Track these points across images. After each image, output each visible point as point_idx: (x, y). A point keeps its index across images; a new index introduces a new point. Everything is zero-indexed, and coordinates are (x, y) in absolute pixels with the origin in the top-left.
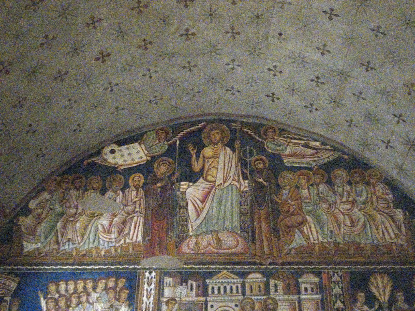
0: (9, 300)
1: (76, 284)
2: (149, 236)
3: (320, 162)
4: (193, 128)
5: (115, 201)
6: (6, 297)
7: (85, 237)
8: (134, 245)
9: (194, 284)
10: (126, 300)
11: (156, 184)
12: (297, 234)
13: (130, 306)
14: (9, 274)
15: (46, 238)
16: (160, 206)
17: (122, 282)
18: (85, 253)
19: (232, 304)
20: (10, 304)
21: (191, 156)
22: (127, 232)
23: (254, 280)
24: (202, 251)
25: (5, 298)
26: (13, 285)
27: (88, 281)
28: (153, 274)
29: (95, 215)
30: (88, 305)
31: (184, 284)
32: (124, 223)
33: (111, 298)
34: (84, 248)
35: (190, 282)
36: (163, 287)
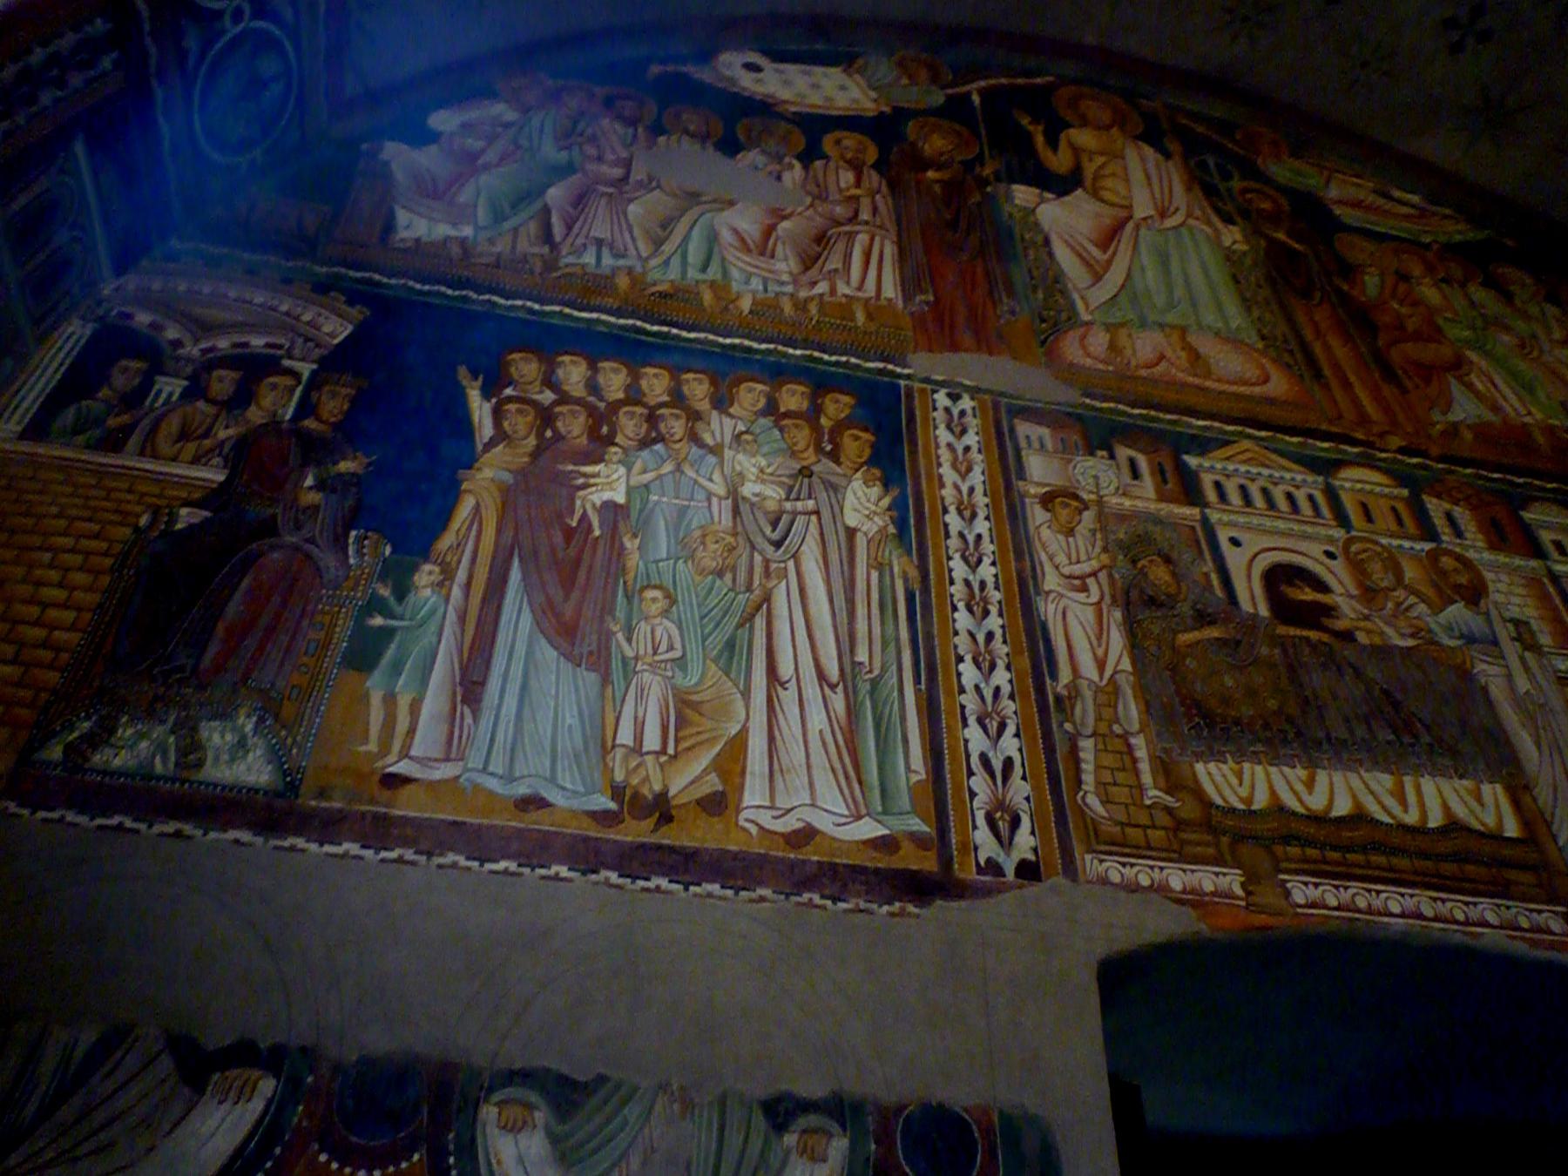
0: (306, 375)
1: (635, 376)
5: (779, 178)
6: (290, 357)
7: (668, 248)
8: (875, 309)
9: (1143, 462)
10: (872, 461)
11: (926, 170)
13: (886, 485)
14: (322, 288)
15: (498, 217)
16: (953, 225)
17: (837, 406)
18: (671, 291)
19: (1317, 549)
20: (315, 383)
21: (1028, 138)
22: (834, 263)
23: (1368, 487)
24: (1143, 373)
25: (287, 363)
26: (336, 329)
27: (690, 376)
28: (966, 403)
29: (704, 199)
31: (1104, 453)
32: (821, 239)
33: (801, 446)
34: (663, 275)
36: (1018, 451)
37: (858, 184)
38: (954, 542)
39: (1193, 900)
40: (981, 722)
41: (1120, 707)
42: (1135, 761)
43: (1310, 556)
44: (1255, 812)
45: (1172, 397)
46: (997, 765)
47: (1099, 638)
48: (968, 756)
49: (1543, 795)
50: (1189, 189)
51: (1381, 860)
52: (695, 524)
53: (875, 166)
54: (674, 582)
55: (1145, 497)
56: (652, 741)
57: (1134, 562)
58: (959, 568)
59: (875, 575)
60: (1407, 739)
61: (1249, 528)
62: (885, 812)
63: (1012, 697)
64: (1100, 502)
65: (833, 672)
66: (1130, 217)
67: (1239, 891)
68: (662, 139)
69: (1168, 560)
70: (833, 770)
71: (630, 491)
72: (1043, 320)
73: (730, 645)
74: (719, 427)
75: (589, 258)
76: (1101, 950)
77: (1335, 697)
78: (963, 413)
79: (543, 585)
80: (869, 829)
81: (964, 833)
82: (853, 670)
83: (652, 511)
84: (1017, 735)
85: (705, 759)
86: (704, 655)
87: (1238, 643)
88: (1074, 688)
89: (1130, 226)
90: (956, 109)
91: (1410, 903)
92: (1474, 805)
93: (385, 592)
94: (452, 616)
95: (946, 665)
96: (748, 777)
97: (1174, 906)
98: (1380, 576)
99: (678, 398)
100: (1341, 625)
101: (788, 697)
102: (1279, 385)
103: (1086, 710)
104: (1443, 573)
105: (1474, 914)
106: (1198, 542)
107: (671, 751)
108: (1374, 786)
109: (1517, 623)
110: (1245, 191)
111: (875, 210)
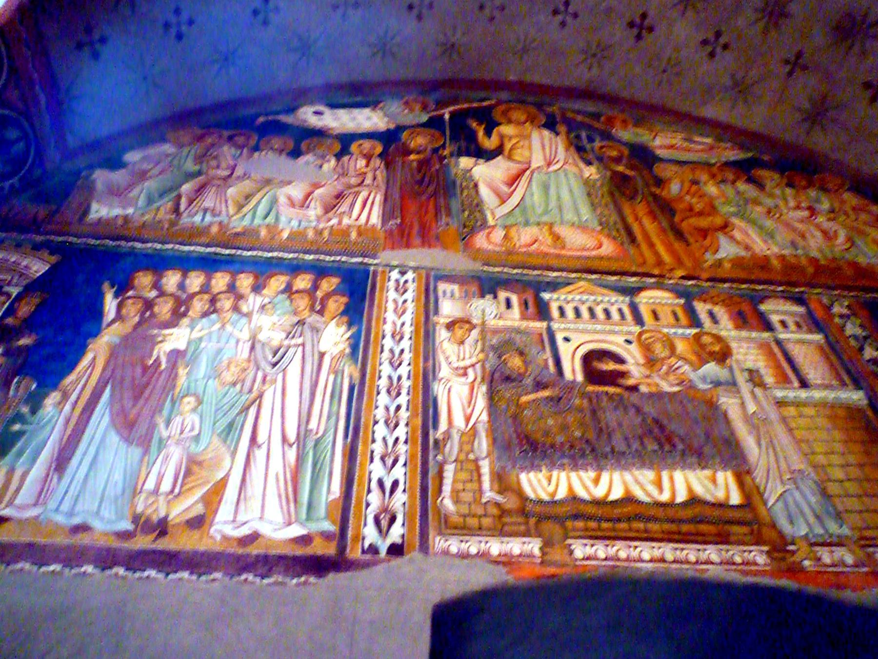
1: (209, 278)
2: (393, 217)
3: (724, 160)
4: (475, 105)
5: (321, 167)
7: (245, 210)
9: (514, 299)
12: (723, 240)
13: (350, 325)
15: (150, 201)
16: (420, 182)
19: (620, 339)
22: (344, 207)
26: (38, 267)
28: (410, 275)
30: (235, 316)
32: (339, 196)
34: (238, 224)
35: (503, 295)
37: (367, 166)
38: (386, 355)
39: (506, 561)
40: (383, 459)
41: (476, 443)
42: (480, 475)
43: (615, 343)
44: (556, 502)
45: (539, 261)
46: (388, 485)
47: (470, 403)
48: (370, 481)
49: (759, 475)
50: (567, 150)
51: (641, 526)
52: (225, 358)
53: (380, 155)
54: (204, 392)
55: (514, 318)
56: (166, 486)
57: (500, 357)
58: (386, 369)
59: (332, 377)
60: (667, 448)
61: (577, 330)
62: (309, 518)
63: (406, 442)
64: (483, 323)
65: (292, 436)
66: (530, 167)
67: (537, 552)
68: (256, 154)
69: (521, 354)
70: (280, 496)
71: (189, 343)
72: (465, 226)
73: (230, 425)
74: (253, 302)
75: (197, 219)
76: (436, 598)
77: (620, 425)
78: (406, 282)
79: (121, 399)
80: (296, 531)
81: (358, 528)
82: (305, 434)
83: (201, 352)
84: (405, 465)
85: (199, 493)
86: (213, 433)
87: (560, 399)
88: (448, 435)
89: (528, 172)
90: (435, 123)
91: (657, 553)
92: (710, 486)
93: (25, 410)
94: (61, 421)
95: (366, 428)
96: (223, 503)
97: (491, 567)
98: (660, 351)
99: (232, 288)
100: (631, 382)
101: (260, 454)
102: (608, 248)
103: (452, 449)
104: (702, 346)
105: (703, 556)
106: (542, 341)
107: (177, 491)
108: (640, 478)
109: (750, 371)
110: (602, 147)
111: (375, 178)
